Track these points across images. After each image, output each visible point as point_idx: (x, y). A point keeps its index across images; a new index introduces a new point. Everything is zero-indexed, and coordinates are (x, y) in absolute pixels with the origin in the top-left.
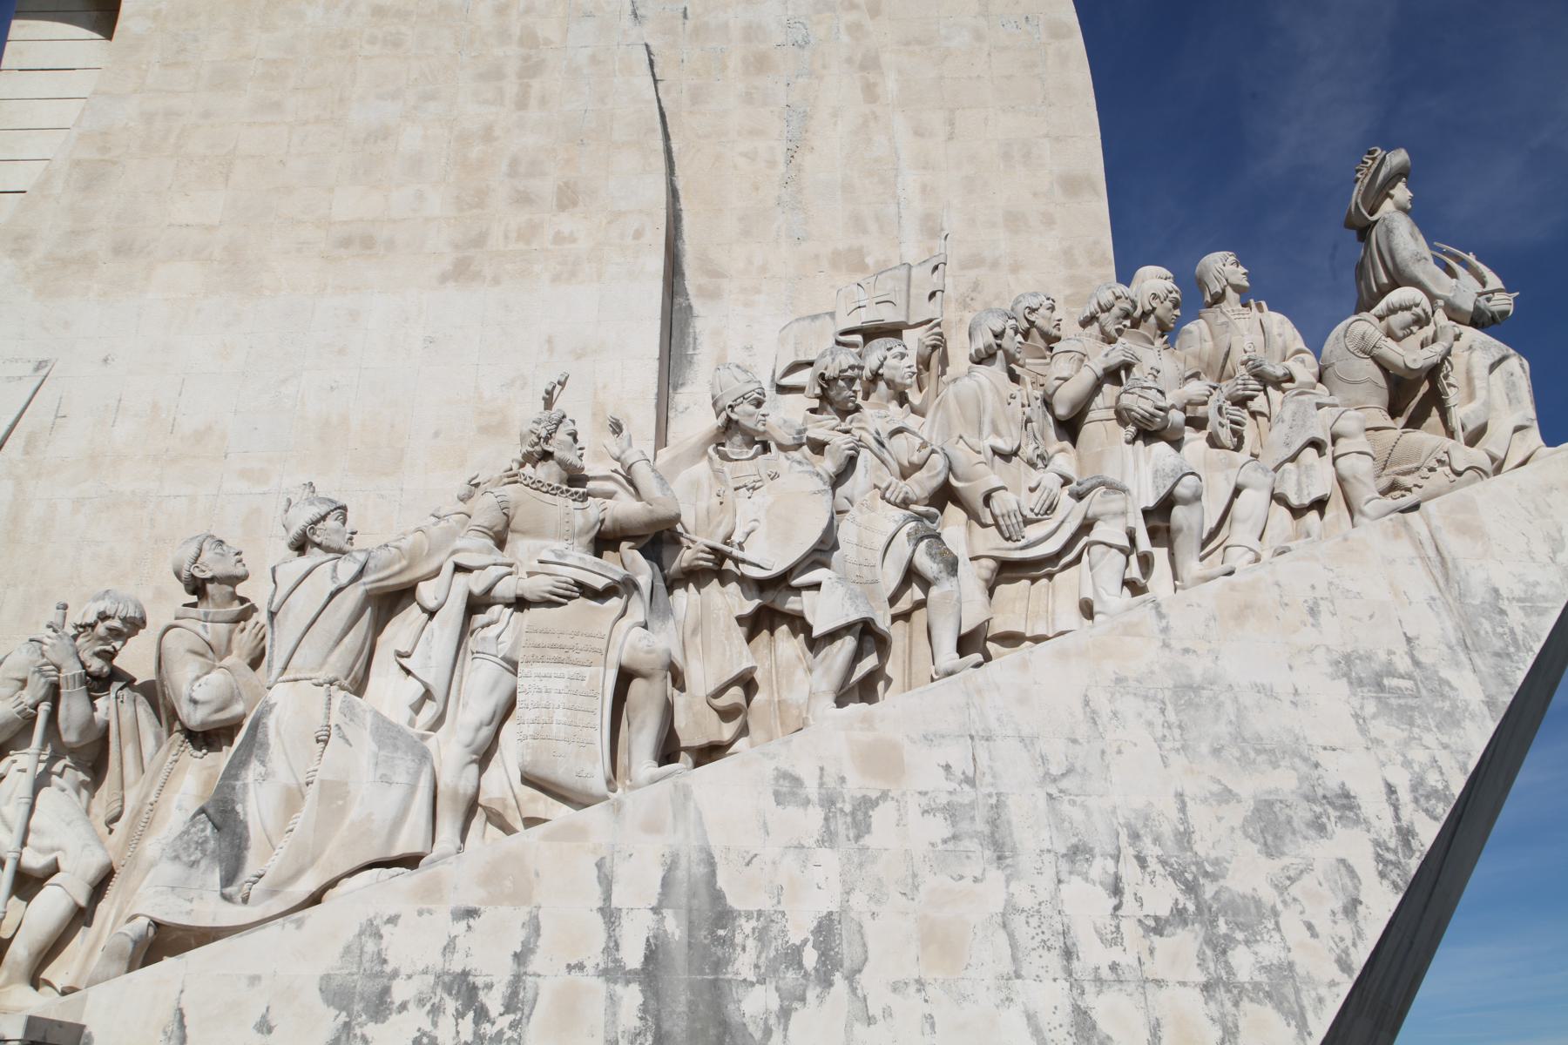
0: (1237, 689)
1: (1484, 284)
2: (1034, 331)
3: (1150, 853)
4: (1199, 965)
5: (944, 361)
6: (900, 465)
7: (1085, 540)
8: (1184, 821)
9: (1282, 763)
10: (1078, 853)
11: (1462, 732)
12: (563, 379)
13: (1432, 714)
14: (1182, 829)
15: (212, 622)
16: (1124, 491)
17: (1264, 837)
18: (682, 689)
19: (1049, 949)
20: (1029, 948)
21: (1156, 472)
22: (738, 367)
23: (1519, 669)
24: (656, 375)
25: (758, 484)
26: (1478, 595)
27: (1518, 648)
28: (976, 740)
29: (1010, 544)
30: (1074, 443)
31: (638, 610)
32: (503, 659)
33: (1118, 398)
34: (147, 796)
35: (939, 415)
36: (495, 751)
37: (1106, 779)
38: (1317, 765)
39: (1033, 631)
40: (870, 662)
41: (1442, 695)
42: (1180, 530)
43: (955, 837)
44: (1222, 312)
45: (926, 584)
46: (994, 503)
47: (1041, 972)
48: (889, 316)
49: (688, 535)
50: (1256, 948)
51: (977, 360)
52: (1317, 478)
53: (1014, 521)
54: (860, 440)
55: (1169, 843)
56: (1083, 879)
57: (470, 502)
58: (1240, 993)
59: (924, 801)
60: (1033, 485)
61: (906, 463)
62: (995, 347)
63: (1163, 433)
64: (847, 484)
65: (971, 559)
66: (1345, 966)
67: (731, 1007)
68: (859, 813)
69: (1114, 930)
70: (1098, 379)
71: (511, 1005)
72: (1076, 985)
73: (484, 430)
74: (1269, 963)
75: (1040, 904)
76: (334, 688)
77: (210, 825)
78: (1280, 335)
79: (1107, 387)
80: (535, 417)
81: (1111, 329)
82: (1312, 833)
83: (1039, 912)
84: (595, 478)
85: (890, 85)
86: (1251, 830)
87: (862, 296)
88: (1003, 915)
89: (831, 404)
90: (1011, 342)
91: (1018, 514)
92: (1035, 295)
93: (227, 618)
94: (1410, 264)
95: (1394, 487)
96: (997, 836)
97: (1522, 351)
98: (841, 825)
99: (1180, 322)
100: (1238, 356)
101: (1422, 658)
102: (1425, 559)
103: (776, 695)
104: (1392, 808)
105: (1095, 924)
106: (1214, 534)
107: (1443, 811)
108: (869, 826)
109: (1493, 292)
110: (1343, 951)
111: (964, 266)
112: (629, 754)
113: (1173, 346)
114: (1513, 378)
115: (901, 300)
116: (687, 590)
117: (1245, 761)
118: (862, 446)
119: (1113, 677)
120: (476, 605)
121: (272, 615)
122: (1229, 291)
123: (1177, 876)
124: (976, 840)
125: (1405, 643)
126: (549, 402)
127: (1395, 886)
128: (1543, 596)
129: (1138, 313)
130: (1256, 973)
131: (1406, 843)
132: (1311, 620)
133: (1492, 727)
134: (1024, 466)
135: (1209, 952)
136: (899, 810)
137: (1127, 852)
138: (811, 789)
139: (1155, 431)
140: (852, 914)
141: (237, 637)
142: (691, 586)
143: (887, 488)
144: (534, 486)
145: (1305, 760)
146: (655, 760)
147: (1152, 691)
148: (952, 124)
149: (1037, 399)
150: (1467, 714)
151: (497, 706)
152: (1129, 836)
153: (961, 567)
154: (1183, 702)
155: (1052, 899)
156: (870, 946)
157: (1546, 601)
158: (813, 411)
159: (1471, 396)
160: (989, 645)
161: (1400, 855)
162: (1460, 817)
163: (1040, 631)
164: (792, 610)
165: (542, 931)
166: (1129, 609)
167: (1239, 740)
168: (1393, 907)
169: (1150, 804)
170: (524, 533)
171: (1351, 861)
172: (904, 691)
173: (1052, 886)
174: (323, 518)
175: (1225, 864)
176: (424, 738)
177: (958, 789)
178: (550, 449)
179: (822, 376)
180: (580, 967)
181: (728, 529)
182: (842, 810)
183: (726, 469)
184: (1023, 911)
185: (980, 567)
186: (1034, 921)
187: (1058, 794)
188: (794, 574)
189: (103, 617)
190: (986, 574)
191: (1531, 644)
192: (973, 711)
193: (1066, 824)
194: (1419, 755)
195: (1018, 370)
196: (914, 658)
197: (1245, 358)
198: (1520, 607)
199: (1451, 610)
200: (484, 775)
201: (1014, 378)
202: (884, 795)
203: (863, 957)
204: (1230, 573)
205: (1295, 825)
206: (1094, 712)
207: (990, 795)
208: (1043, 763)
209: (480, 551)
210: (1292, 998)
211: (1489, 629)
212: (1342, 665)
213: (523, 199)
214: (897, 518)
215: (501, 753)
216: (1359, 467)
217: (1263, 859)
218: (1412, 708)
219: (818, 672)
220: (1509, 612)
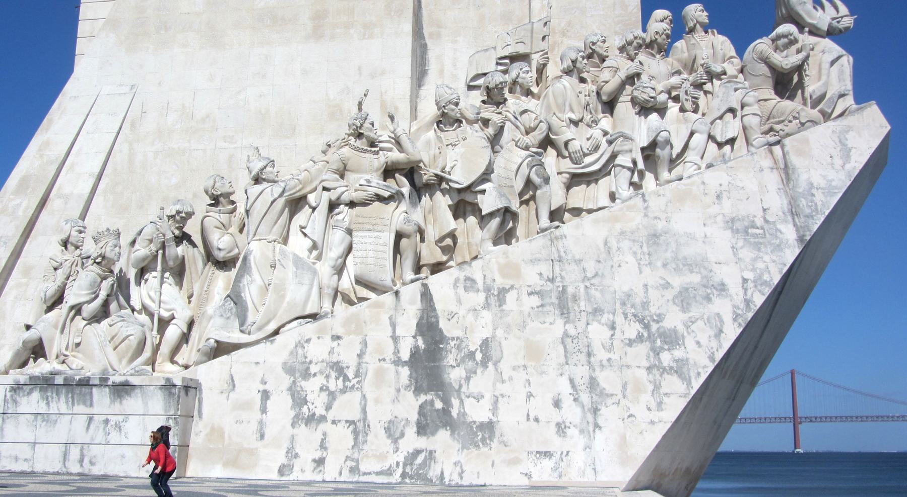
9: (695, 270)
10: (597, 311)
15: (222, 213)
19: (581, 353)
31: (403, 206)
33: (632, 92)
34: (203, 287)
38: (711, 271)
43: (542, 306)
47: (577, 362)
50: (673, 352)
52: (731, 128)
66: (712, 359)
67: (446, 376)
70: (623, 81)
71: (357, 375)
76: (276, 243)
77: (232, 303)
82: (705, 302)
83: (578, 337)
86: (676, 301)
87: (509, 40)
88: (562, 339)
93: (229, 211)
95: (771, 130)
98: (493, 301)
99: (670, 45)
100: (700, 61)
109: (842, 17)
117: (677, 270)
118: (507, 120)
120: (333, 206)
121: (247, 212)
123: (641, 321)
127: (740, 325)
135: (652, 354)
138: (480, 284)
139: (652, 107)
140: (497, 339)
141: (233, 219)
145: (705, 268)
149: (593, 92)
152: (621, 304)
156: (504, 351)
162: (780, 293)
165: (368, 345)
168: (738, 334)
169: (631, 290)
173: (584, 326)
174: (265, 167)
176: (314, 263)
180: (384, 360)
183: (442, 136)
189: (178, 212)
194: (760, 265)
197: (703, 62)
198: (823, 193)
207: (559, 287)
210: (686, 373)
211: (805, 204)
216: (752, 121)
217: (680, 313)
218: (761, 243)
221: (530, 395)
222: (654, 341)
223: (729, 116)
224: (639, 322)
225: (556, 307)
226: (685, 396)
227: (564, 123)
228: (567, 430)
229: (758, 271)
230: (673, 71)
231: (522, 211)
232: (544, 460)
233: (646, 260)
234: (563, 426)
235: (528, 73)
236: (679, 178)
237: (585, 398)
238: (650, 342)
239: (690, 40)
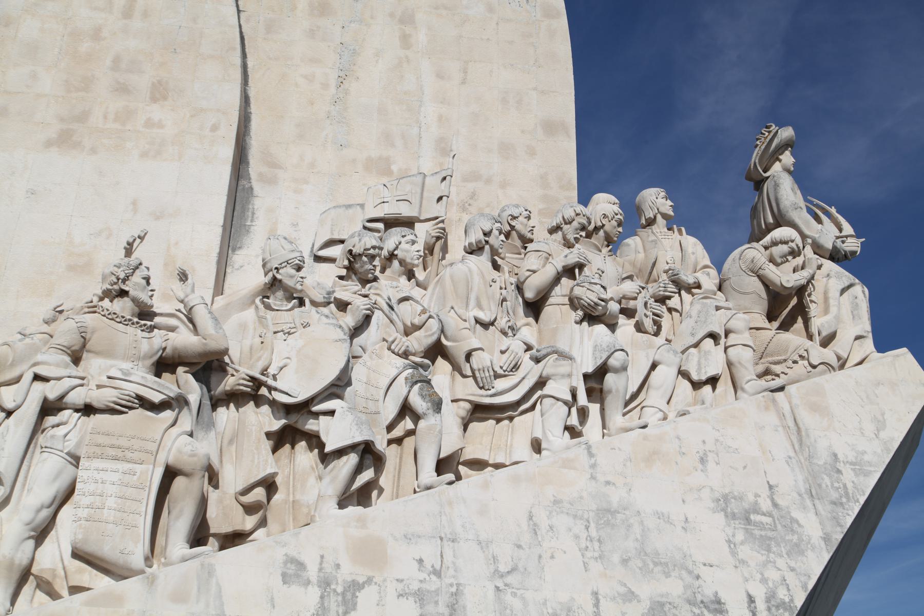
0: (643, 515)
1: (841, 230)
2: (514, 233)
5: (445, 249)
6: (405, 325)
7: (539, 393)
9: (673, 574)
11: (805, 559)
12: (142, 235)
13: (784, 544)
16: (571, 359)
18: (216, 487)
21: (596, 345)
22: (285, 238)
23: (849, 515)
24: (219, 239)
25: (293, 331)
26: (823, 458)
28: (445, 540)
29: (483, 392)
30: (537, 320)
31: (186, 421)
32: (68, 454)
33: (572, 289)
35: (437, 289)
36: (52, 530)
37: (541, 577)
38: (698, 577)
39: (495, 459)
40: (367, 475)
41: (792, 530)
42: (610, 392)
44: (652, 232)
45: (416, 417)
46: (474, 360)
48: (406, 211)
49: (233, 366)
51: (470, 251)
53: (487, 374)
54: (375, 304)
57: (53, 325)
59: (400, 586)
60: (504, 348)
61: (409, 324)
62: (484, 242)
63: (603, 318)
64: (363, 336)
65: (452, 401)
68: (348, 593)
70: (558, 273)
73: (71, 268)
78: (693, 253)
79: (564, 280)
80: (117, 262)
81: (571, 237)
84: (161, 315)
85: (421, 37)
87: (386, 194)
89: (355, 274)
90: (496, 240)
91: (491, 369)
92: (517, 206)
94: (790, 210)
95: (767, 372)
97: (864, 281)
99: (623, 237)
100: (661, 266)
101: (780, 501)
102: (786, 427)
103: (291, 496)
106: (634, 396)
108: (356, 604)
109: (847, 237)
111: (466, 179)
112: (167, 536)
113: (615, 254)
114: (856, 300)
115: (415, 200)
116: (228, 408)
118: (376, 308)
119: (552, 500)
120: (48, 408)
122: (659, 217)
126: (129, 251)
128: (869, 462)
129: (591, 228)
132: (700, 466)
133: (827, 557)
134: (498, 334)
136: (380, 593)
138: (312, 572)
139: (597, 316)
142: (232, 405)
143: (393, 342)
144: (110, 317)
145: (690, 572)
146: (188, 542)
147: (580, 513)
148: (465, 72)
149: (512, 284)
150: (809, 546)
151: (57, 492)
153: (444, 407)
154: (602, 522)
157: (871, 466)
158: (341, 278)
159: (826, 311)
160: (461, 468)
163: (499, 460)
164: (311, 430)
166: (568, 448)
167: (642, 554)
169: (573, 599)
170: (98, 353)
172: (392, 500)
177: (428, 579)
178: (127, 289)
179: (350, 252)
181: (266, 363)
182: (335, 591)
183: (268, 317)
185: (459, 407)
187: (504, 587)
188: (314, 403)
190: (463, 413)
191: (858, 497)
192: (444, 518)
193: (508, 611)
194: (773, 575)
195: (500, 261)
196: (402, 474)
197: (667, 268)
198: (852, 469)
199: (802, 467)
200: (39, 549)
201: (496, 267)
202: (369, 581)
204: (644, 427)
206: (535, 525)
207: (451, 585)
208: (494, 562)
209: (57, 365)
211: (829, 484)
213: (122, 89)
214: (398, 366)
215: (56, 531)
218: (770, 539)
219: (326, 480)
220: (844, 471)
223: (709, 341)
227: (467, 323)
229: (771, 584)
230: (624, 276)
231: (391, 454)
233: (594, 550)
235: (413, 245)
236: (642, 425)
239: (649, 236)
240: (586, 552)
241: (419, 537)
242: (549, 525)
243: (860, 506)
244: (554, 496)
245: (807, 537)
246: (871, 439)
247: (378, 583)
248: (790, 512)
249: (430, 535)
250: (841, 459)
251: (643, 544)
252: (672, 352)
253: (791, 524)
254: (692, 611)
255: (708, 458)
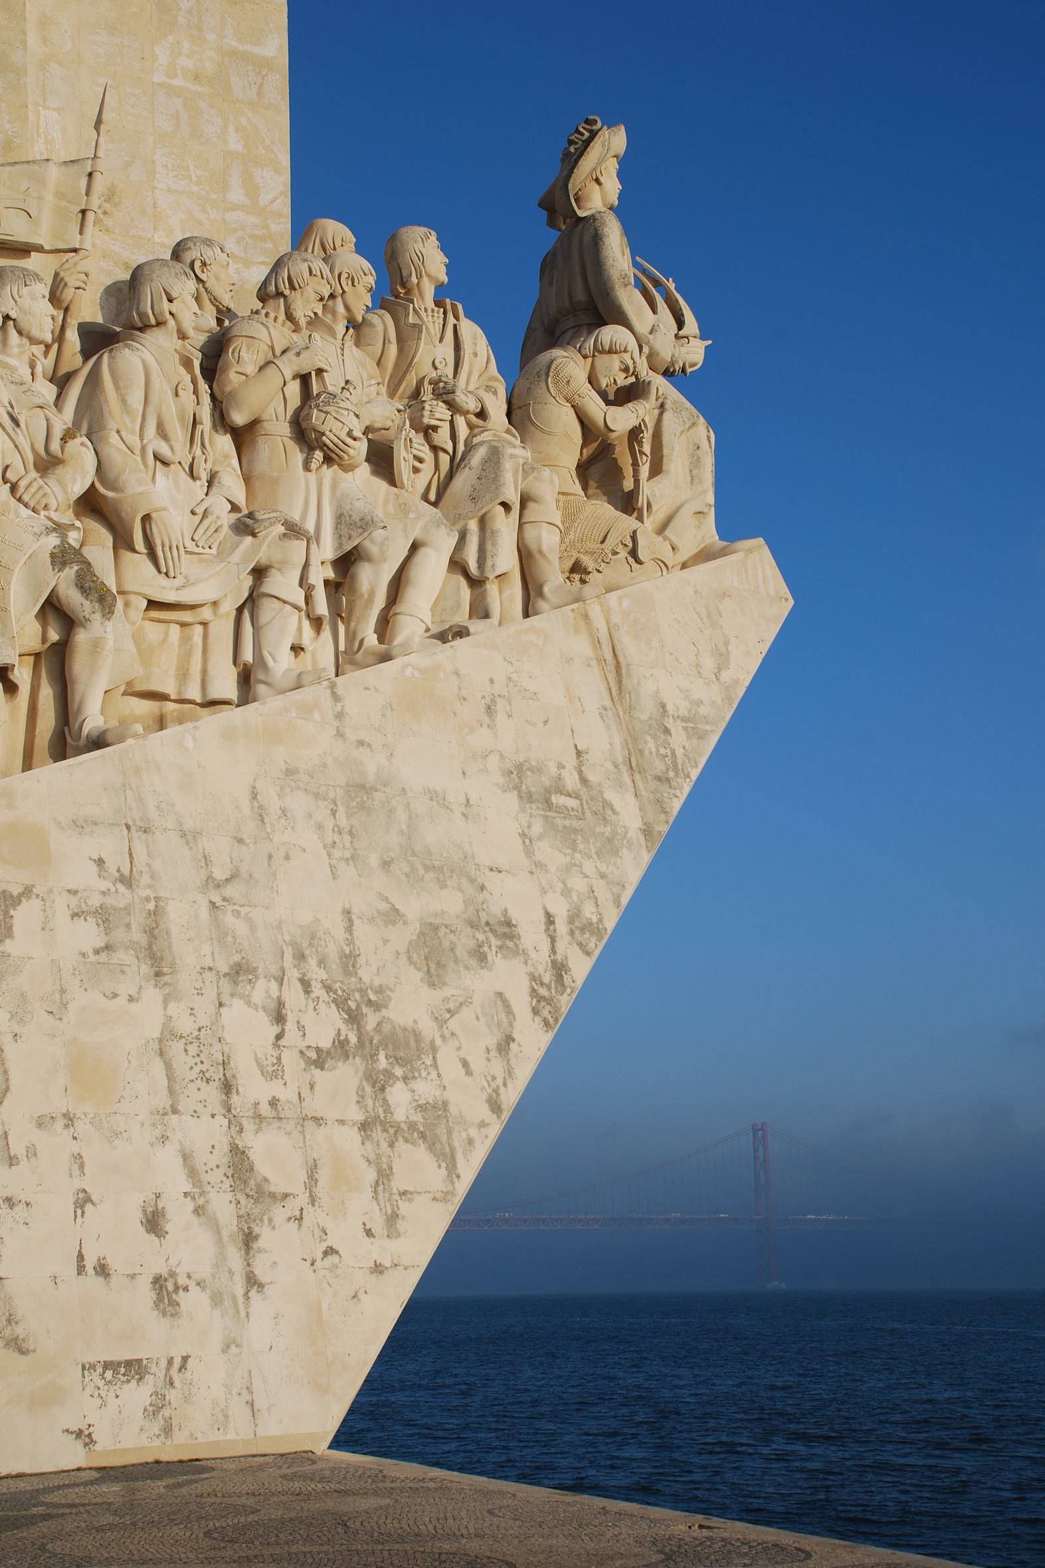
0: (410, 794)
3: (314, 976)
4: (358, 1102)
8: (350, 942)
9: (449, 883)
10: (240, 972)
11: (619, 861)
13: (594, 840)
14: (348, 952)
17: (428, 964)
19: (208, 1081)
20: (187, 1080)
23: (676, 796)
26: (646, 712)
27: (677, 775)
28: (133, 829)
38: (482, 888)
41: (604, 819)
43: (108, 947)
47: (199, 1107)
55: (334, 967)
56: (246, 1003)
58: (396, 1132)
59: (73, 901)
66: (495, 1107)
69: (275, 1061)
72: (235, 1123)
74: (424, 1102)
75: (199, 1030)
82: (473, 963)
86: (415, 956)
88: (160, 1041)
96: (154, 948)
97: (711, 422)
101: (591, 777)
102: (601, 661)
104: (550, 940)
105: (256, 1054)
107: (597, 946)
108: (10, 928)
110: (494, 1091)
119: (284, 767)
123: (340, 1003)
124: (132, 952)
125: (575, 756)
127: (546, 1023)
128: (705, 718)
130: (413, 1111)
131: (559, 979)
132: (487, 720)
133: (646, 858)
135: (368, 1089)
137: (293, 974)
145: (472, 881)
147: (323, 789)
150: (625, 842)
152: (294, 954)
154: (354, 804)
155: (212, 1024)
157: (707, 723)
161: (553, 991)
167: (409, 854)
169: (317, 921)
171: (508, 995)
173: (212, 1009)
175: (388, 992)
184: (181, 1037)
186: (193, 1050)
187: (222, 903)
191: (689, 769)
192: (129, 794)
193: (229, 939)
194: (578, 884)
198: (683, 727)
199: (621, 724)
202: (28, 892)
203: (4, 1087)
205: (458, 952)
206: (261, 807)
207: (147, 899)
208: (207, 865)
210: (444, 1138)
211: (654, 750)
212: (514, 776)
218: (576, 831)
220: (672, 732)
221: (83, 1201)
222: (372, 1056)
224: (337, 1005)
225: (141, 956)
226: (445, 1197)
228: (181, 1296)
229: (575, 898)
232: (125, 1386)
233: (344, 847)
234: (171, 1287)
237: (222, 1204)
238: (363, 1057)
240: (332, 850)
241: (96, 824)
242: (281, 808)
243: (692, 784)
244: (286, 762)
245: (623, 829)
246: (709, 682)
247: (41, 895)
248: (603, 792)
249: (111, 821)
250: (671, 713)
251: (410, 838)
252: (443, 527)
253: (604, 810)
254: (474, 937)
255: (498, 707)
